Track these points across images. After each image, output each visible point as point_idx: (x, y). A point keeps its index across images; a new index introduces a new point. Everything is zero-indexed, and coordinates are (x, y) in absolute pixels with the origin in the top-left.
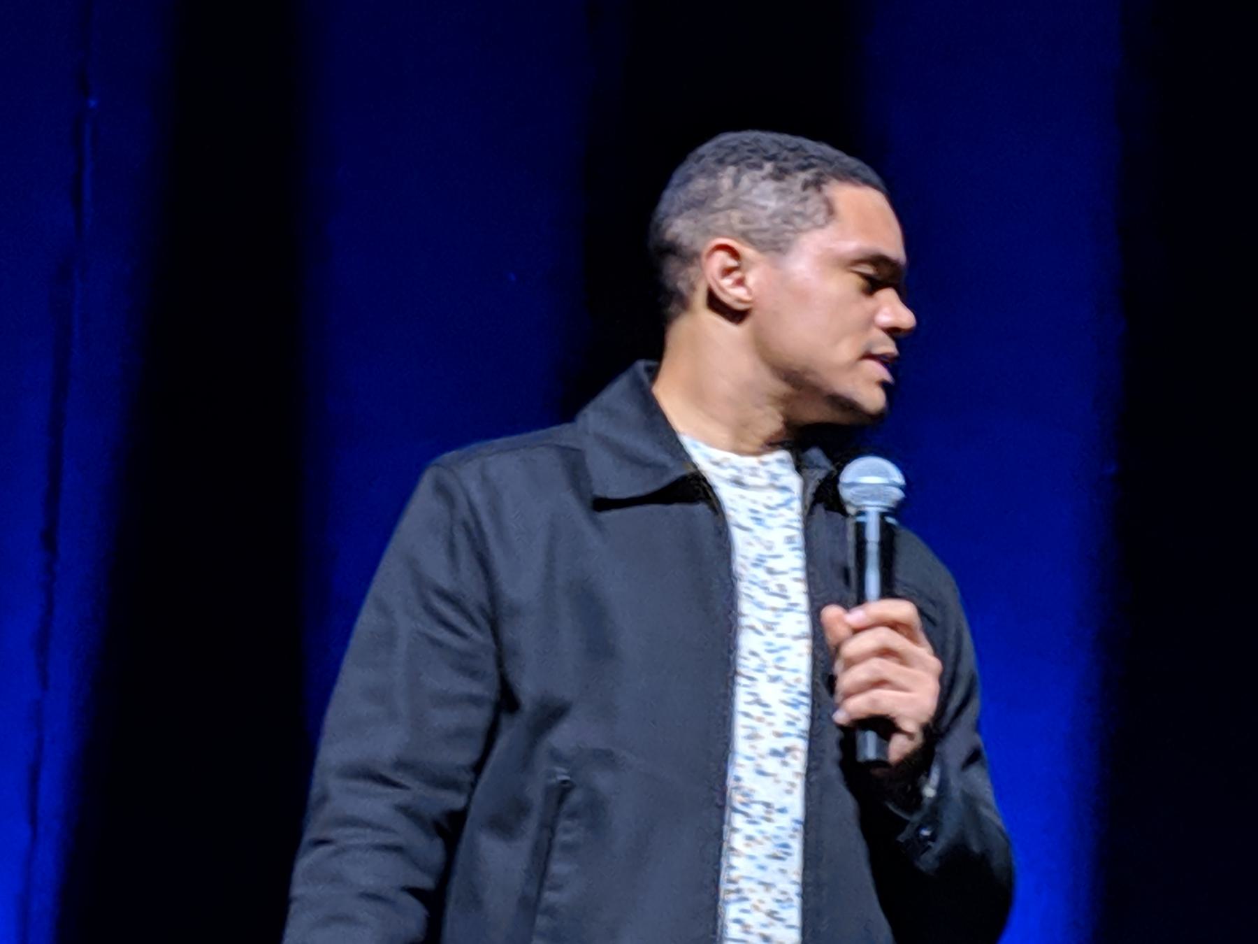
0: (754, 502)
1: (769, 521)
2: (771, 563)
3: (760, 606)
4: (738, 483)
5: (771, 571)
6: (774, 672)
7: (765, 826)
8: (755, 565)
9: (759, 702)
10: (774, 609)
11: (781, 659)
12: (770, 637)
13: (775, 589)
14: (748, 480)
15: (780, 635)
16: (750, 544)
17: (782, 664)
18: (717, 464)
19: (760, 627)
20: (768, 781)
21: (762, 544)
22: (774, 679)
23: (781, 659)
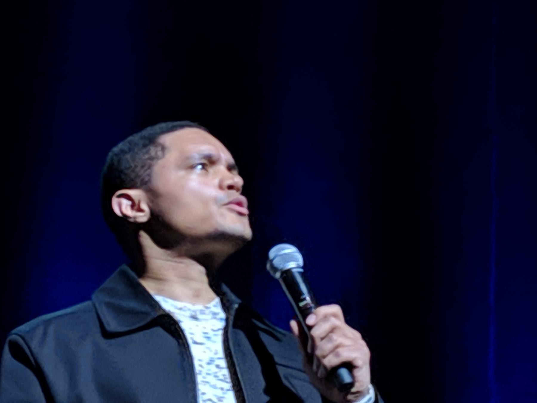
0: (204, 328)
1: (214, 338)
2: (218, 362)
3: (214, 387)
4: (194, 318)
5: (218, 366)
8: (209, 364)
10: (222, 389)
13: (222, 377)
14: (200, 316)
16: (205, 352)
18: (180, 309)
19: (215, 400)
21: (211, 351)
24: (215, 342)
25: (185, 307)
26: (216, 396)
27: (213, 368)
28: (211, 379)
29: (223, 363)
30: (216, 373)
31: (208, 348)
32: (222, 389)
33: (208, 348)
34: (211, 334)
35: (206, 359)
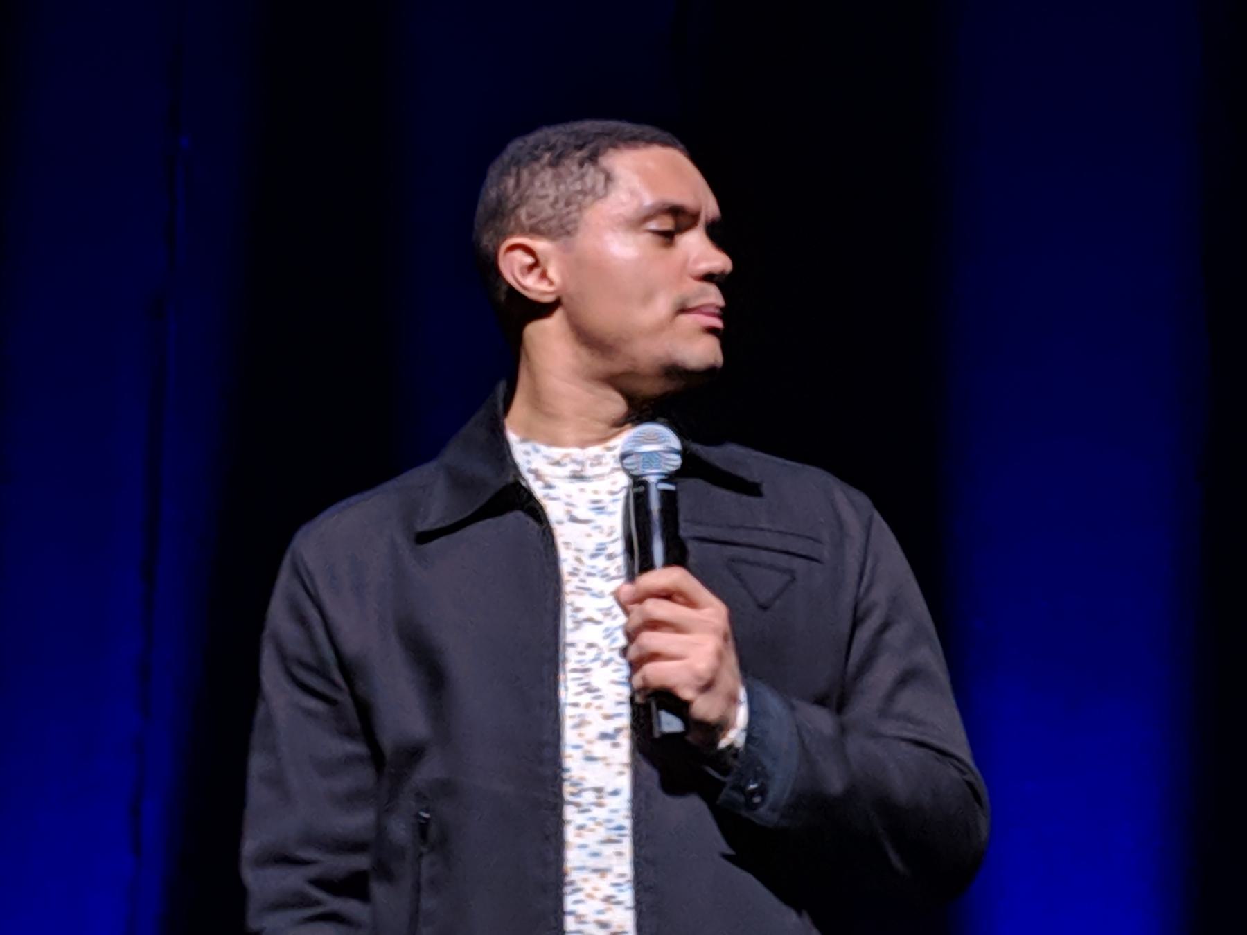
0: (596, 492)
3: (600, 595)
7: (597, 812)
8: (593, 556)
9: (590, 690)
14: (589, 471)
16: (589, 535)
19: (598, 617)
20: (598, 765)
25: (567, 455)
26: (601, 610)
27: (601, 562)
35: (590, 546)
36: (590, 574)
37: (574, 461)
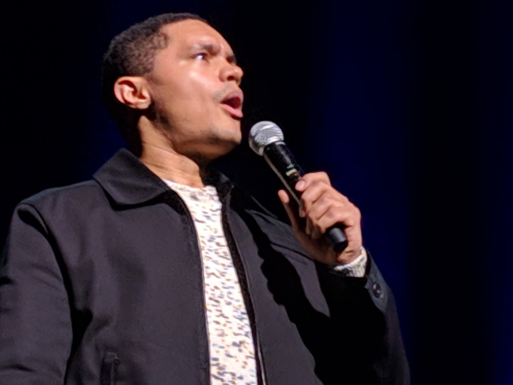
0: (204, 208)
1: (213, 218)
3: (216, 262)
5: (218, 244)
6: (228, 300)
8: (210, 241)
9: (222, 315)
10: (223, 265)
11: (230, 293)
12: (223, 279)
13: (222, 255)
15: (228, 280)
16: (205, 230)
17: (231, 296)
19: (217, 274)
20: (232, 360)
21: (211, 229)
22: (229, 304)
23: (230, 293)
24: (214, 221)
26: (218, 271)
28: (212, 255)
29: (223, 241)
30: (217, 250)
31: (208, 226)
32: (223, 265)
33: (208, 226)
34: (210, 213)
35: (207, 237)
36: (210, 250)
37: (189, 191)
